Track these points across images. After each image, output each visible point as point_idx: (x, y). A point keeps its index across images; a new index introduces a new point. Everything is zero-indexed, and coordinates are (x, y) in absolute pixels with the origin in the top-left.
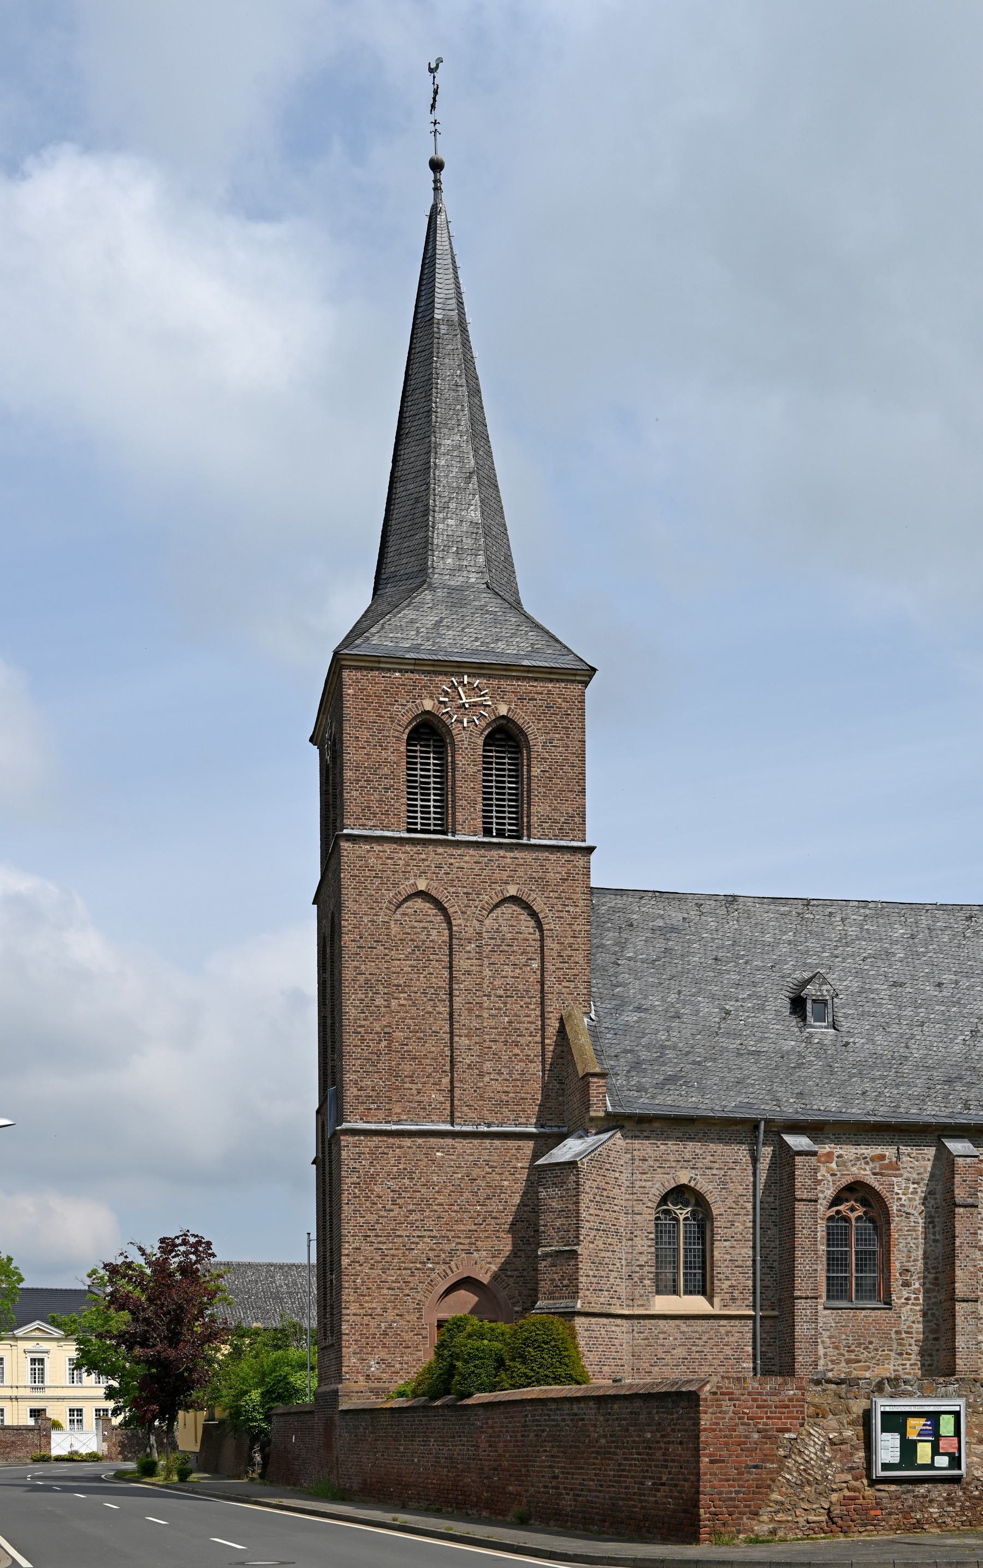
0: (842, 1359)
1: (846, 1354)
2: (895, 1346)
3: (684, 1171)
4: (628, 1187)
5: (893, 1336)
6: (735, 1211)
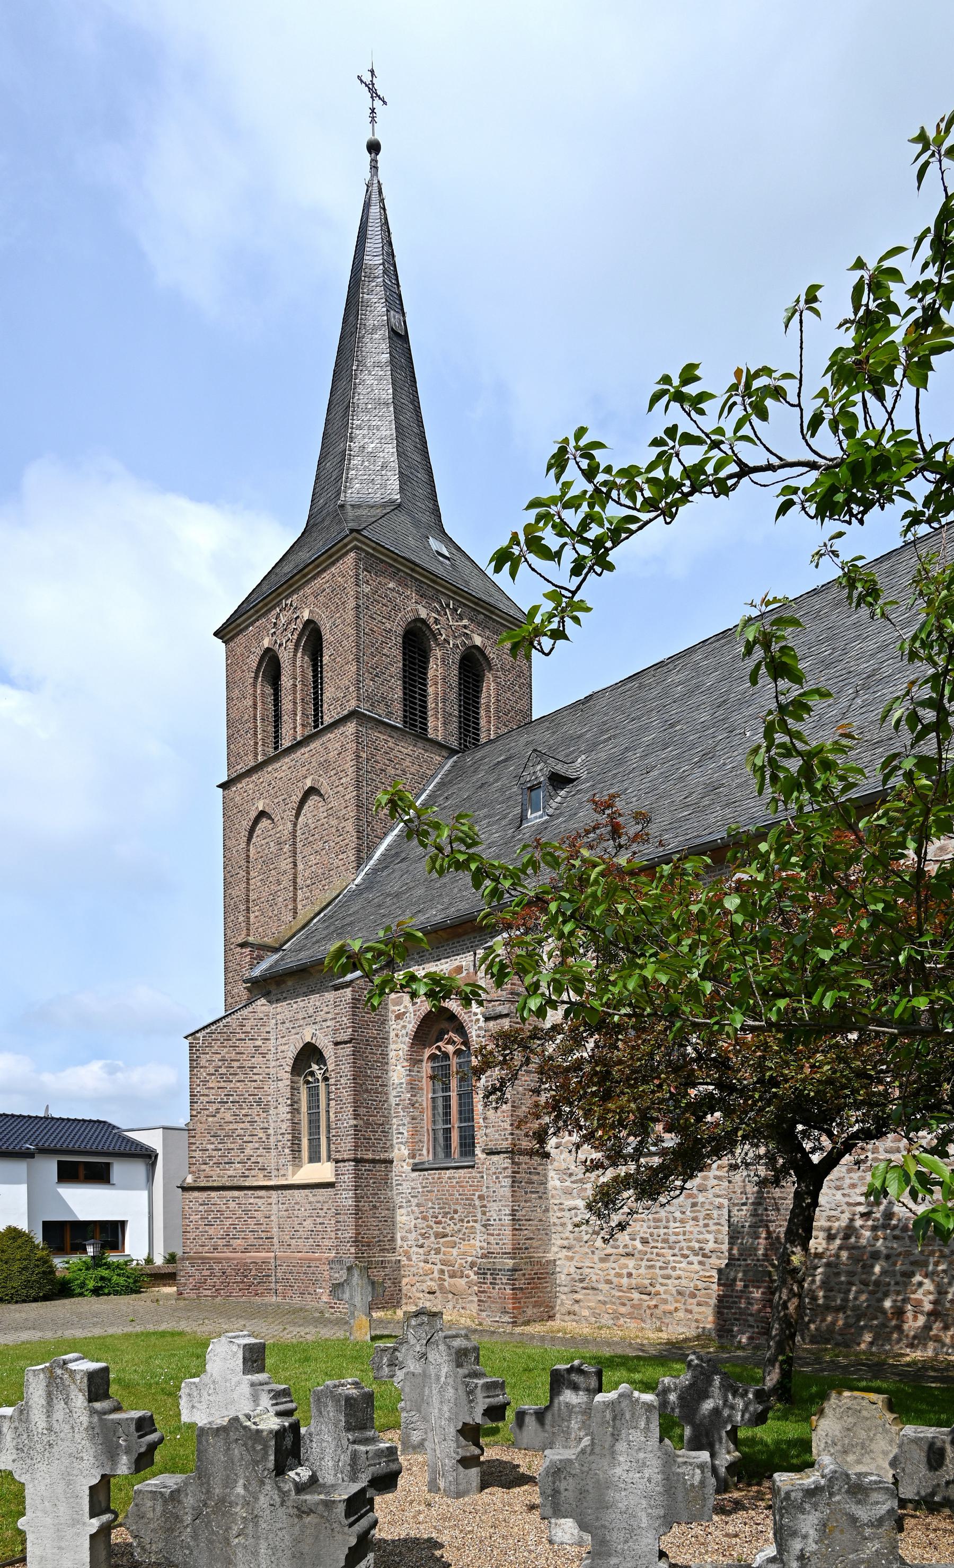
0: (431, 1232)
1: (434, 1226)
2: (479, 1216)
5: (477, 1203)
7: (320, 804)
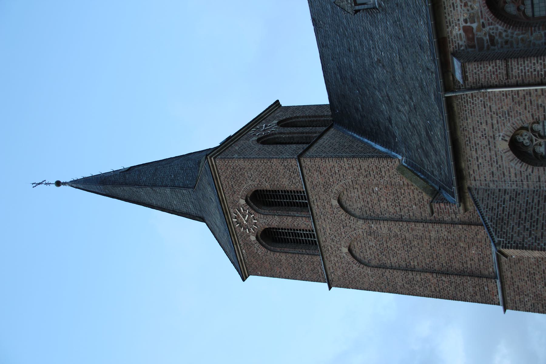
3: (498, 146)
4: (517, 186)
6: (528, 104)
7: (349, 195)
